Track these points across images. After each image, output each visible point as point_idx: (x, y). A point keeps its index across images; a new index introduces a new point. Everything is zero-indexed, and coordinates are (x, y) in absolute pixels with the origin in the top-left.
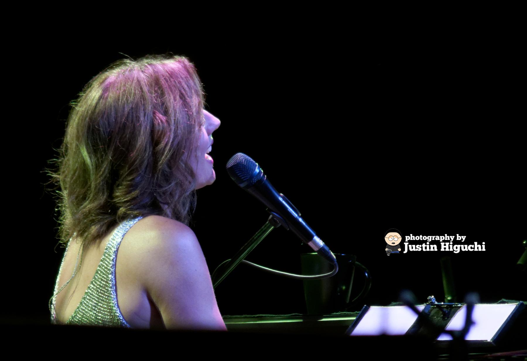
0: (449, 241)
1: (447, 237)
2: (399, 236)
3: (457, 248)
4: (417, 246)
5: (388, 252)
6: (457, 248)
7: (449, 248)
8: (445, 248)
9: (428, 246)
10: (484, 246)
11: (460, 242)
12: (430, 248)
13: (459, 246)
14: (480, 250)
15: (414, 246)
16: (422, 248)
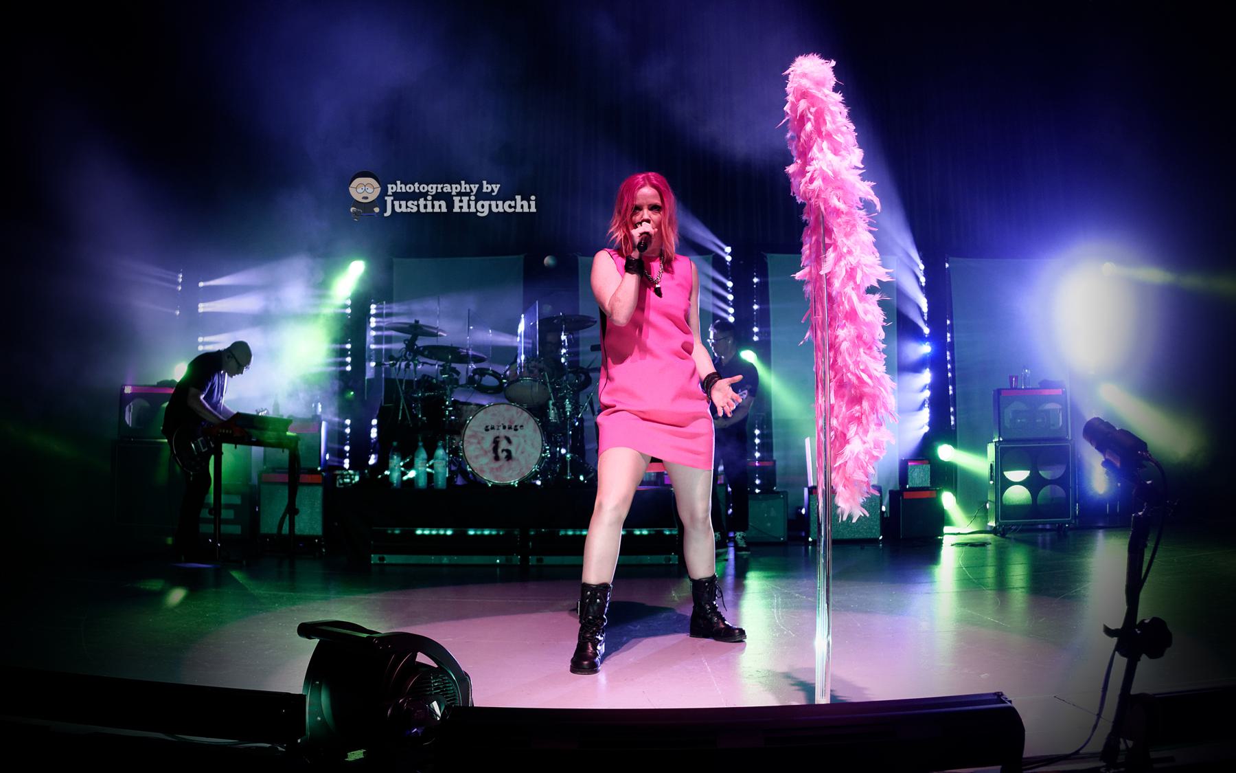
0: (468, 194)
1: (464, 187)
2: (376, 184)
3: (483, 206)
4: (410, 203)
5: (355, 213)
6: (483, 206)
7: (469, 207)
8: (461, 207)
9: (429, 204)
10: (533, 204)
11: (488, 197)
12: (433, 207)
13: (486, 203)
14: (526, 210)
15: (403, 203)
16: (418, 206)
